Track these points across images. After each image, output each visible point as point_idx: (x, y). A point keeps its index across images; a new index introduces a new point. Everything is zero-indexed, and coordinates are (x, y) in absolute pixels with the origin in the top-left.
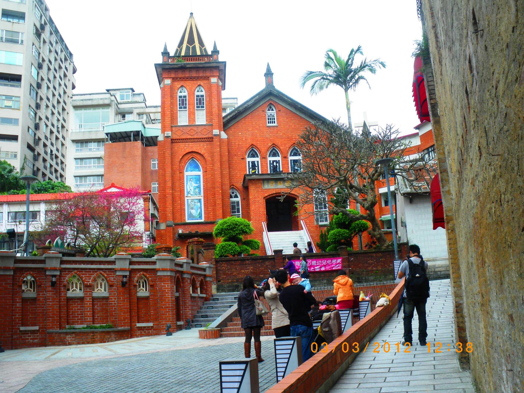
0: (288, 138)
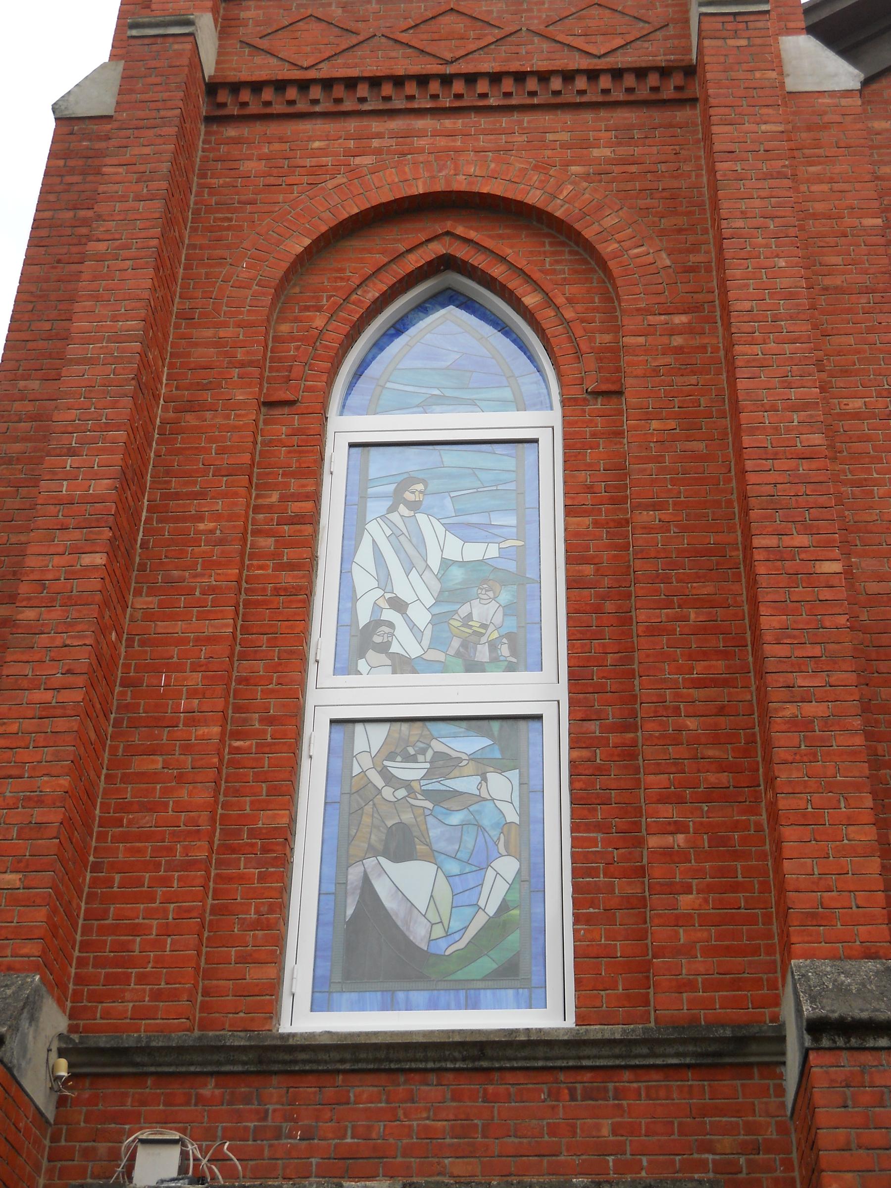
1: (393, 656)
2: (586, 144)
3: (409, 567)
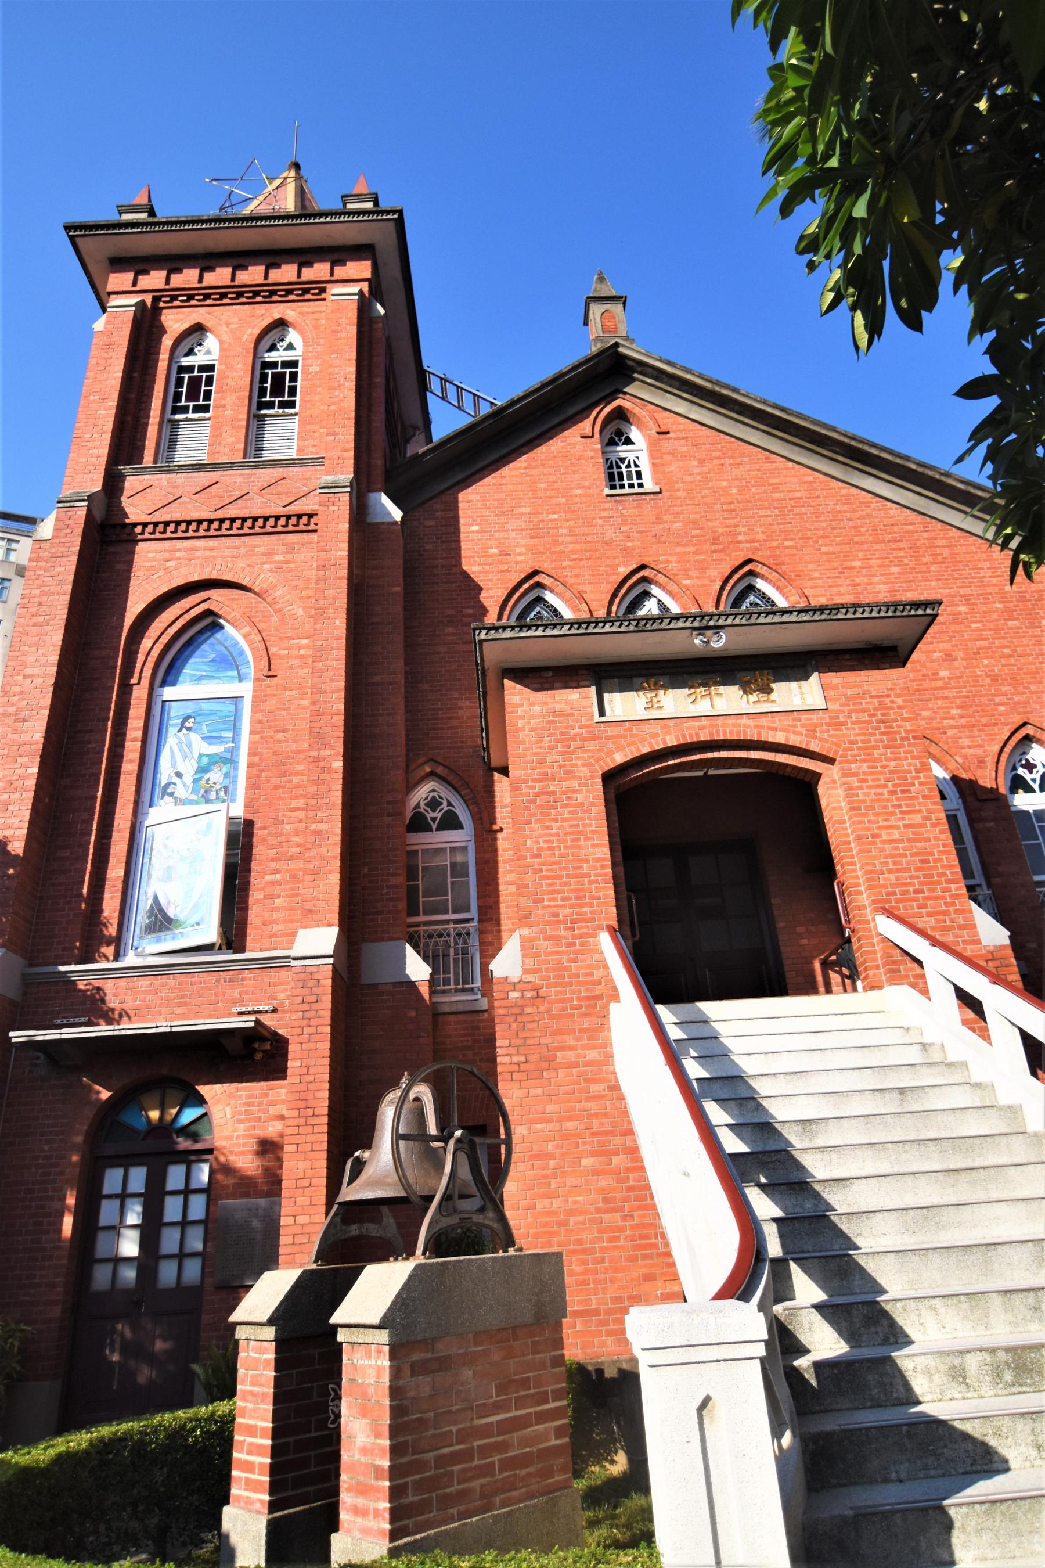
0: (715, 541)
1: (176, 798)
2: (272, 553)
3: (185, 757)
